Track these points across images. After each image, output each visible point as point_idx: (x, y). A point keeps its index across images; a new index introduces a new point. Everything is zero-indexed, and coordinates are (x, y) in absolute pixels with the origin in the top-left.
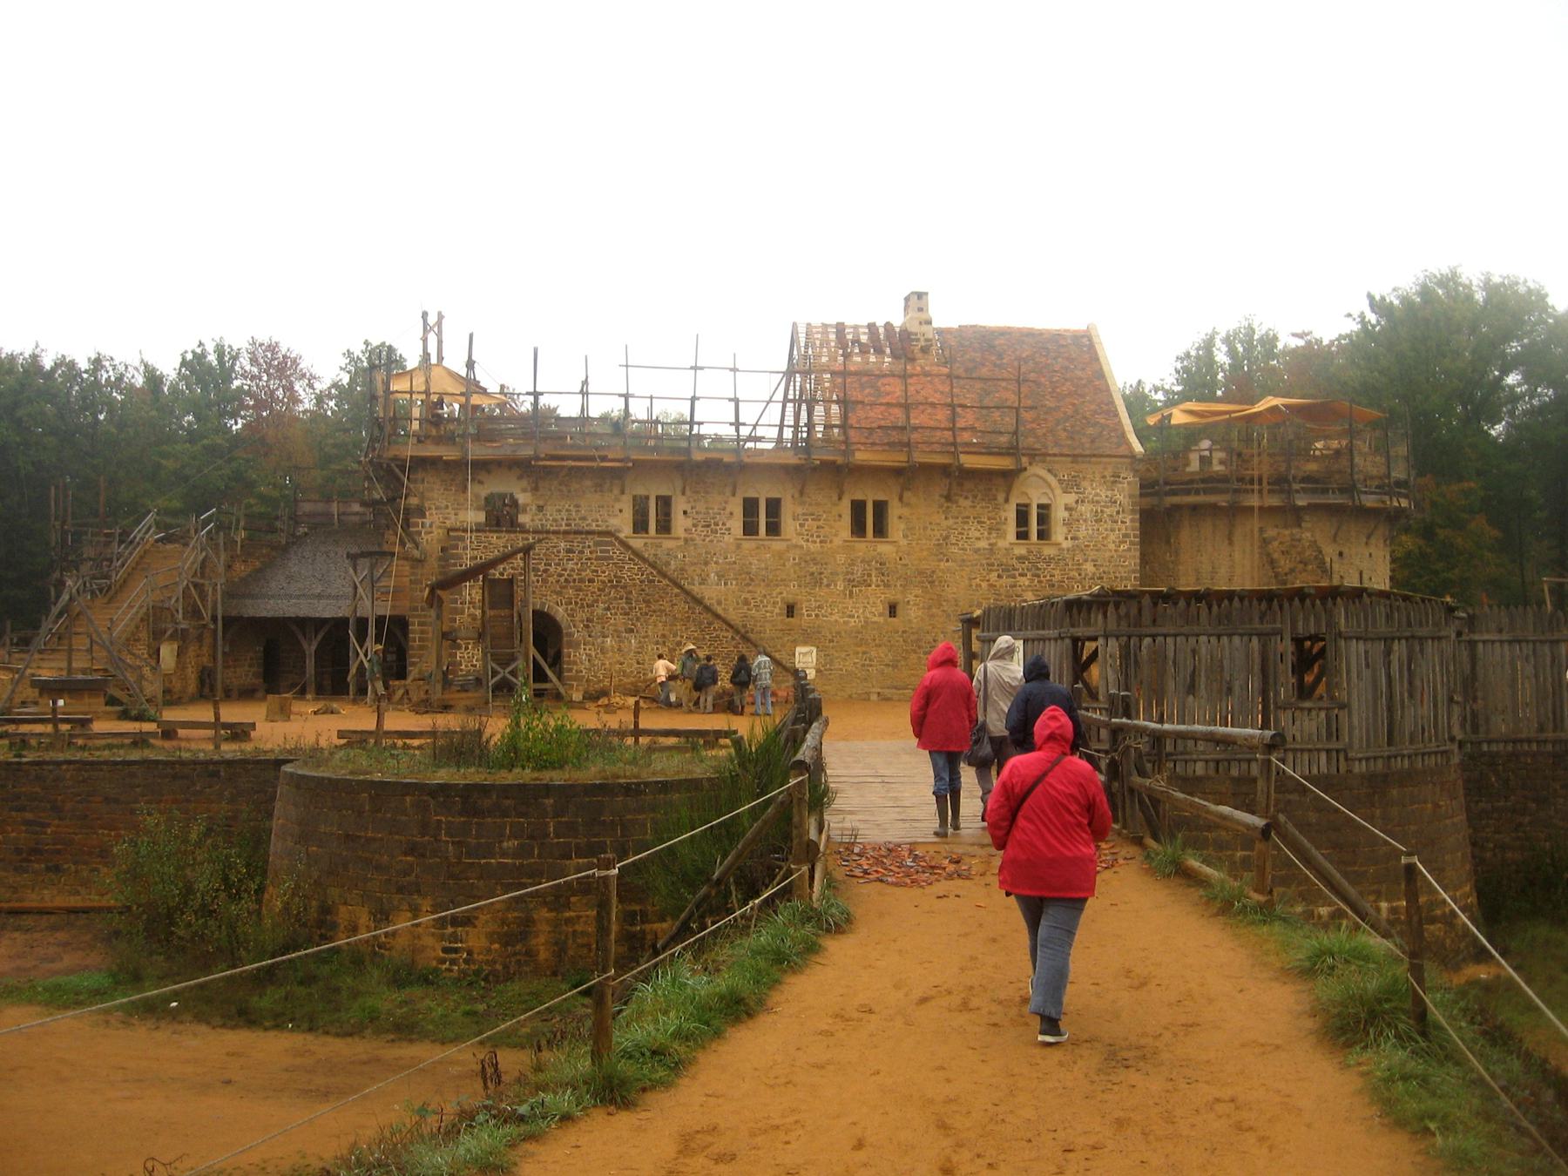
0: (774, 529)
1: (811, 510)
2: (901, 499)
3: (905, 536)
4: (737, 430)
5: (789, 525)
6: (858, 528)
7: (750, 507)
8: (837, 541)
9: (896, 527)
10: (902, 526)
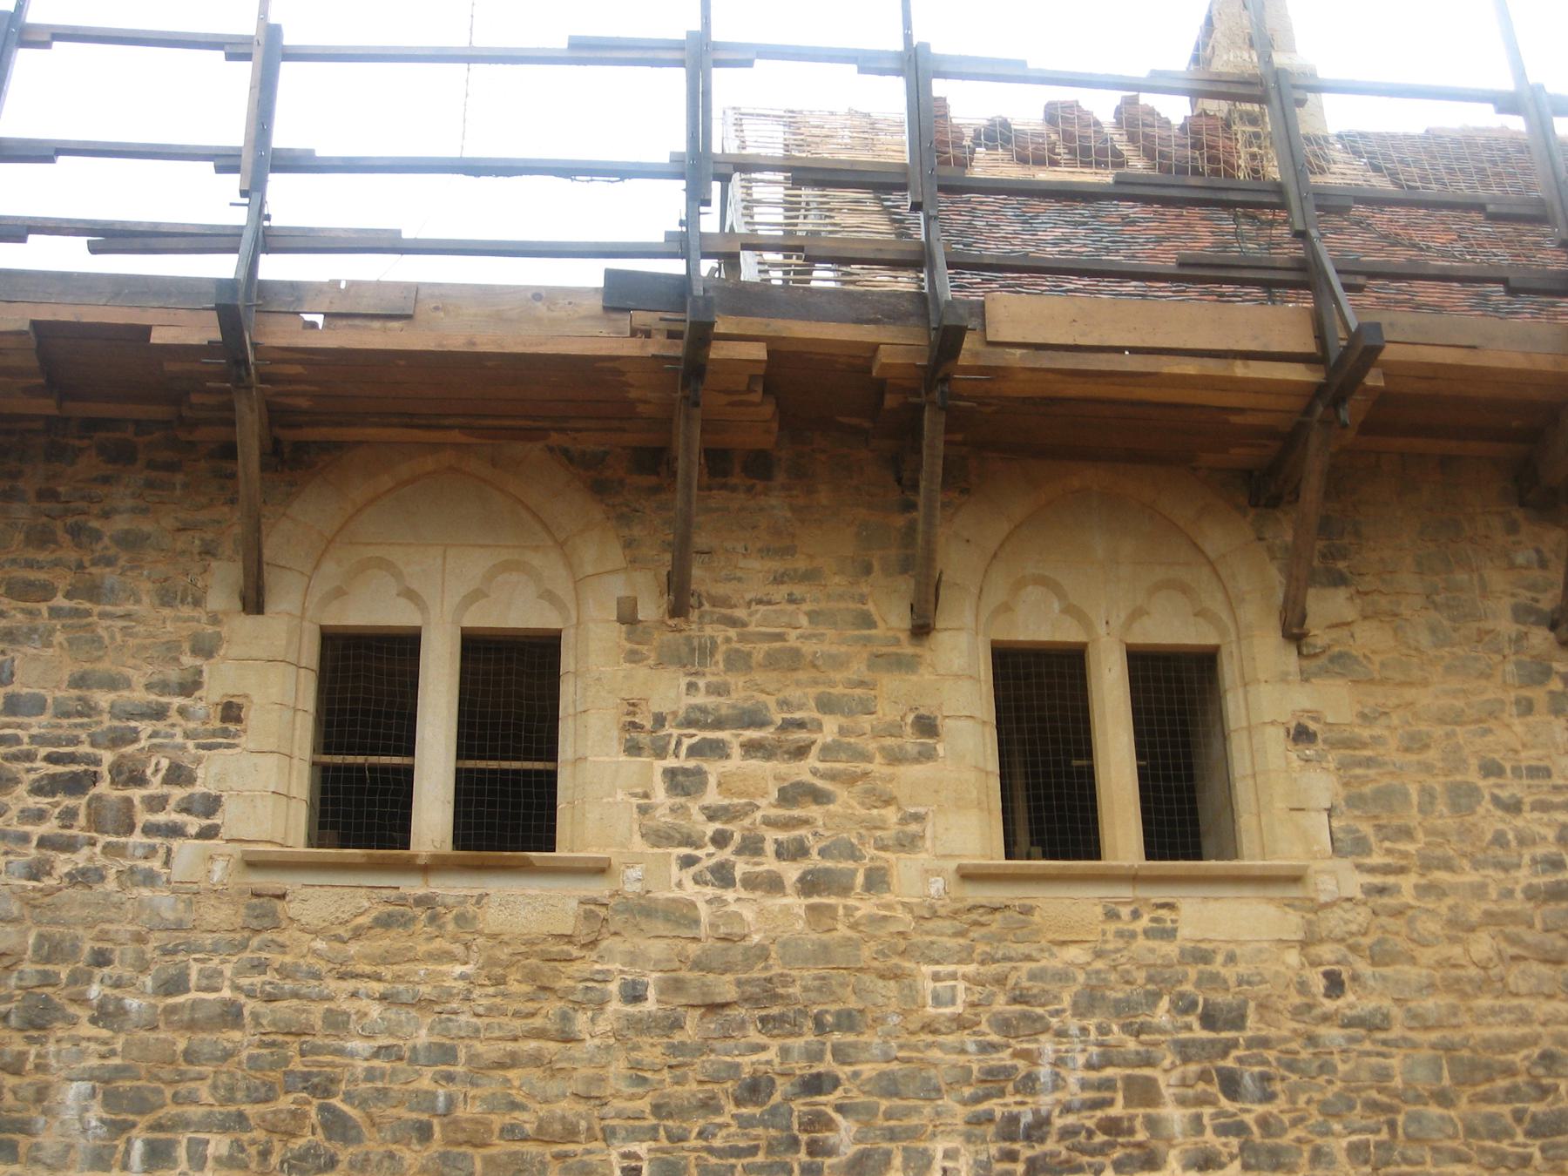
0: (511, 813)
1: (740, 692)
2: (1294, 632)
3: (1346, 846)
4: (253, 191)
5: (600, 782)
6: (1047, 810)
7: (362, 687)
8: (919, 879)
9: (1278, 790)
10: (1322, 786)
